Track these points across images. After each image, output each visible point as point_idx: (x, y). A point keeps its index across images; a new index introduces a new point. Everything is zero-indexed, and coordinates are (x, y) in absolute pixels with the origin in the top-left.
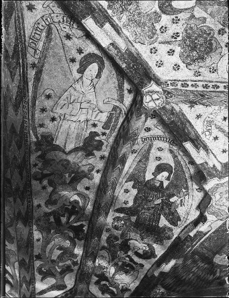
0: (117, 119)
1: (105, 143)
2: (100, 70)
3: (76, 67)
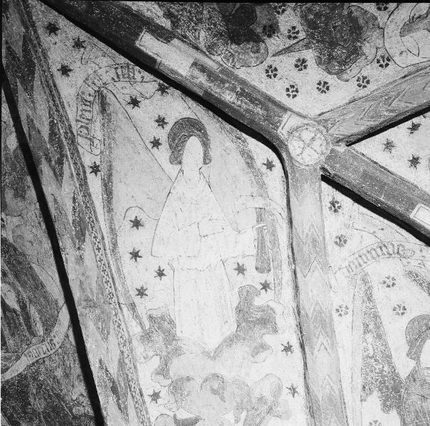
0: (274, 234)
1: (278, 309)
2: (206, 144)
3: (163, 153)
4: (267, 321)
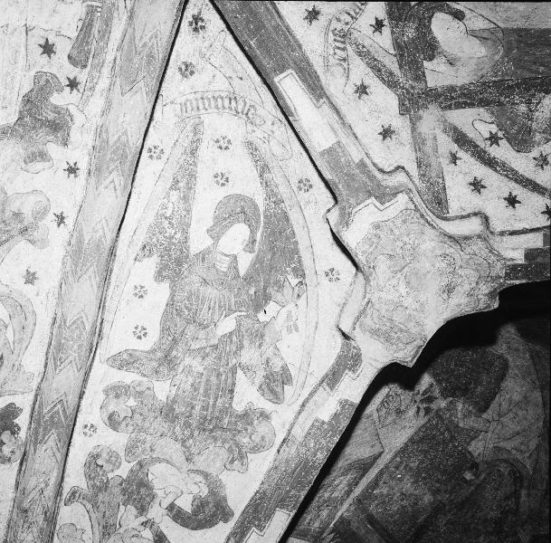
0: (108, 22)
1: (79, 119)
4: (58, 126)
